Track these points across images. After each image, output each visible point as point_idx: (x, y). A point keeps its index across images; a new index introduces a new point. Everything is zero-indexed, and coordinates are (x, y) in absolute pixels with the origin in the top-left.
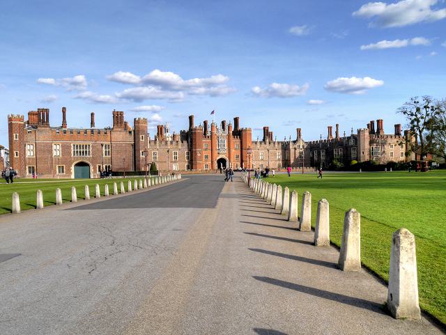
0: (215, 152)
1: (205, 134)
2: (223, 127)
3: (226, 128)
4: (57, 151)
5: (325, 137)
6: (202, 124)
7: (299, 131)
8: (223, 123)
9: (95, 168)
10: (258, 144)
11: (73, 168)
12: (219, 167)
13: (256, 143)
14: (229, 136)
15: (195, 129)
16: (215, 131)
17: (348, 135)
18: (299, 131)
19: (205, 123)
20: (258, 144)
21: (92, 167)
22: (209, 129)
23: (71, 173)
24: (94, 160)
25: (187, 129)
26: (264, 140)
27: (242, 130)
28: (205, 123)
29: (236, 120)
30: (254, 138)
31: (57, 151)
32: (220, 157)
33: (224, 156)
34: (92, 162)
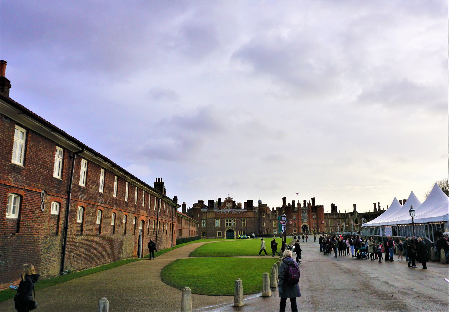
4: (217, 223)
5: (372, 210)
7: (355, 206)
8: (305, 201)
9: (237, 233)
11: (225, 233)
12: (304, 231)
18: (355, 206)
19: (293, 202)
20: (328, 215)
21: (235, 233)
22: (296, 206)
23: (224, 236)
24: (237, 229)
25: (281, 205)
28: (293, 202)
29: (313, 199)
30: (325, 212)
31: (217, 223)
32: (304, 224)
33: (306, 224)
34: (236, 230)
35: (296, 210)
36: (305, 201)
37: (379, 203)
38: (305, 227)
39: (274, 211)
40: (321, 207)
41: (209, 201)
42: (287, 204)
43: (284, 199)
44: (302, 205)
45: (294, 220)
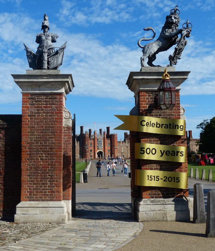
0: (96, 148)
1: (90, 137)
2: (101, 133)
3: (102, 133)
6: (88, 131)
8: (100, 130)
10: (121, 143)
12: (99, 156)
13: (120, 142)
14: (104, 138)
15: (85, 135)
16: (96, 136)
19: (90, 130)
20: (121, 143)
22: (92, 134)
26: (125, 140)
28: (90, 130)
30: (119, 140)
32: (99, 150)
33: (101, 150)
36: (100, 130)
42: (84, 132)
45: (91, 147)
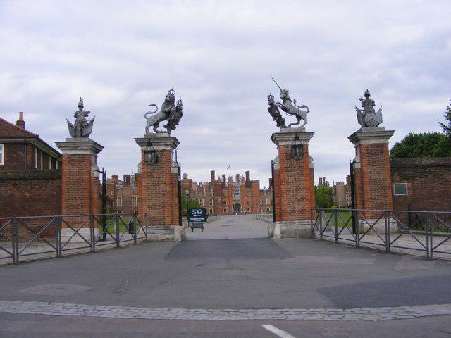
6: (221, 177)
8: (238, 176)
12: (235, 210)
17: (331, 185)
19: (224, 176)
22: (227, 181)
27: (252, 182)
28: (224, 176)
29: (248, 173)
35: (227, 185)
36: (238, 176)
37: (324, 178)
38: (237, 206)
39: (200, 188)
40: (257, 183)
41: (125, 176)
42: (216, 179)
43: (213, 173)
44: (235, 180)
